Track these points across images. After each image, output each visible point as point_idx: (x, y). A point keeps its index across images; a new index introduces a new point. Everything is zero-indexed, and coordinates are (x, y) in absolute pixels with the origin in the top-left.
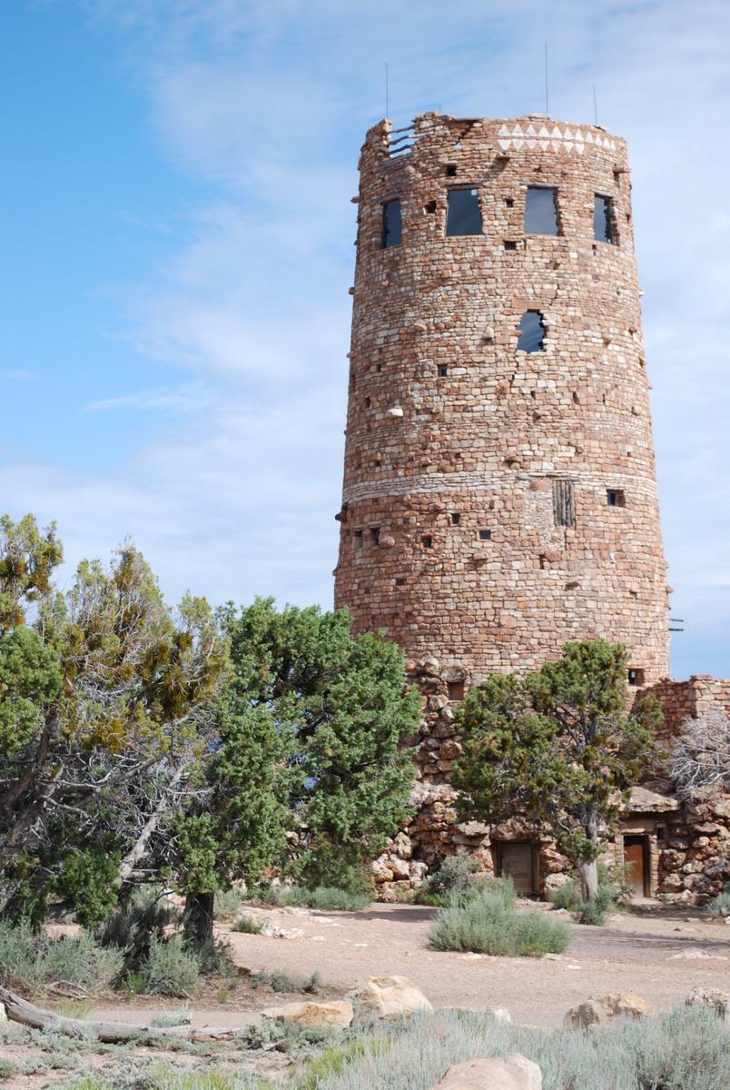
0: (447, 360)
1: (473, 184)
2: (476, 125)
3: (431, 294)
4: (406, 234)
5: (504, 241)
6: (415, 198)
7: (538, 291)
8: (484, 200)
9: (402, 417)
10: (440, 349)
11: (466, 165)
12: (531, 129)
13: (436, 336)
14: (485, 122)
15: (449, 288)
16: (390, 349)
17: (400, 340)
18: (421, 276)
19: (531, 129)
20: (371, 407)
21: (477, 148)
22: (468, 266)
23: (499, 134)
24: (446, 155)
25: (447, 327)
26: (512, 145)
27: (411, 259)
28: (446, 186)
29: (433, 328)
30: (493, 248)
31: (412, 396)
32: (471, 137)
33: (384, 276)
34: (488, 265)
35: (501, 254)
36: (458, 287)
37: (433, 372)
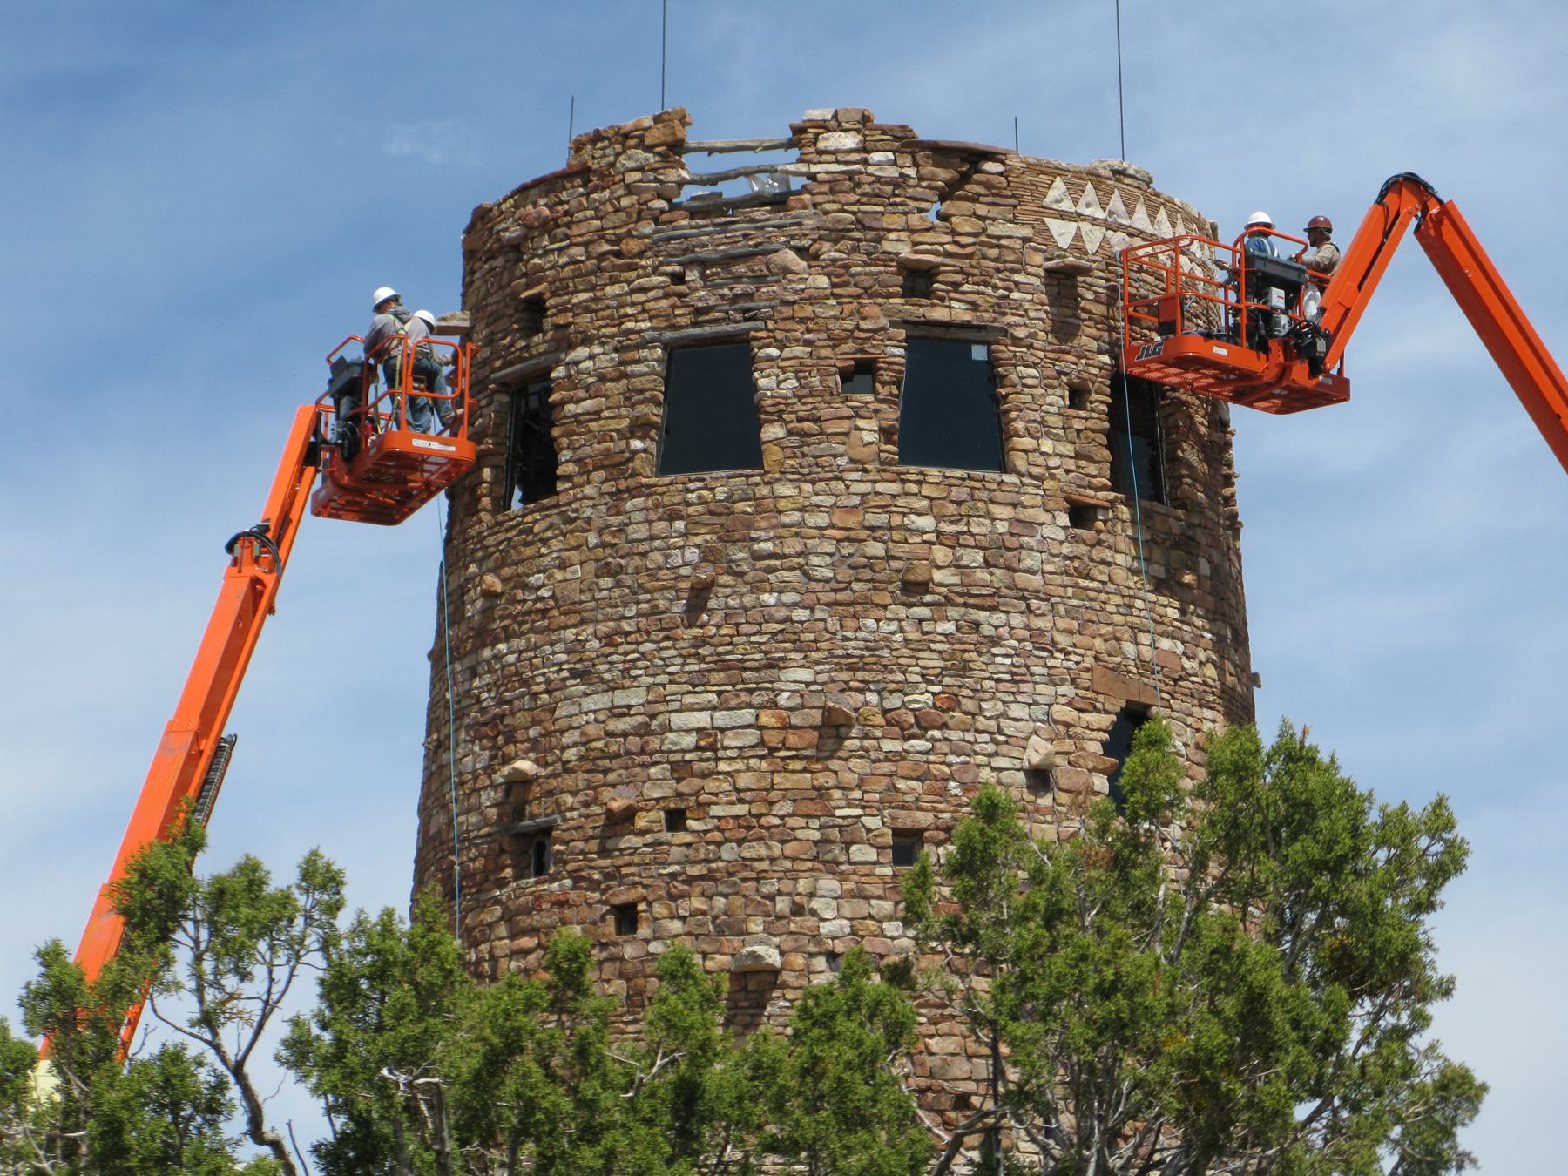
0: (924, 819)
1: (979, 328)
2: (990, 166)
3: (870, 623)
4: (777, 441)
5: (1068, 499)
6: (808, 343)
7: (1147, 653)
8: (1014, 377)
9: (775, 972)
10: (901, 784)
11: (961, 271)
12: (1116, 202)
13: (888, 745)
14: (1013, 162)
15: (925, 612)
16: (723, 766)
17: (762, 743)
18: (833, 566)
19: (1116, 202)
20: (644, 931)
21: (992, 230)
22: (979, 556)
23: (1047, 202)
24: (903, 235)
25: (923, 725)
26: (1078, 237)
27: (796, 517)
28: (905, 323)
29: (880, 720)
30: (1045, 517)
31: (814, 913)
32: (975, 199)
33: (692, 554)
34: (1030, 561)
35: (1061, 535)
36: (954, 612)
37: (880, 848)
